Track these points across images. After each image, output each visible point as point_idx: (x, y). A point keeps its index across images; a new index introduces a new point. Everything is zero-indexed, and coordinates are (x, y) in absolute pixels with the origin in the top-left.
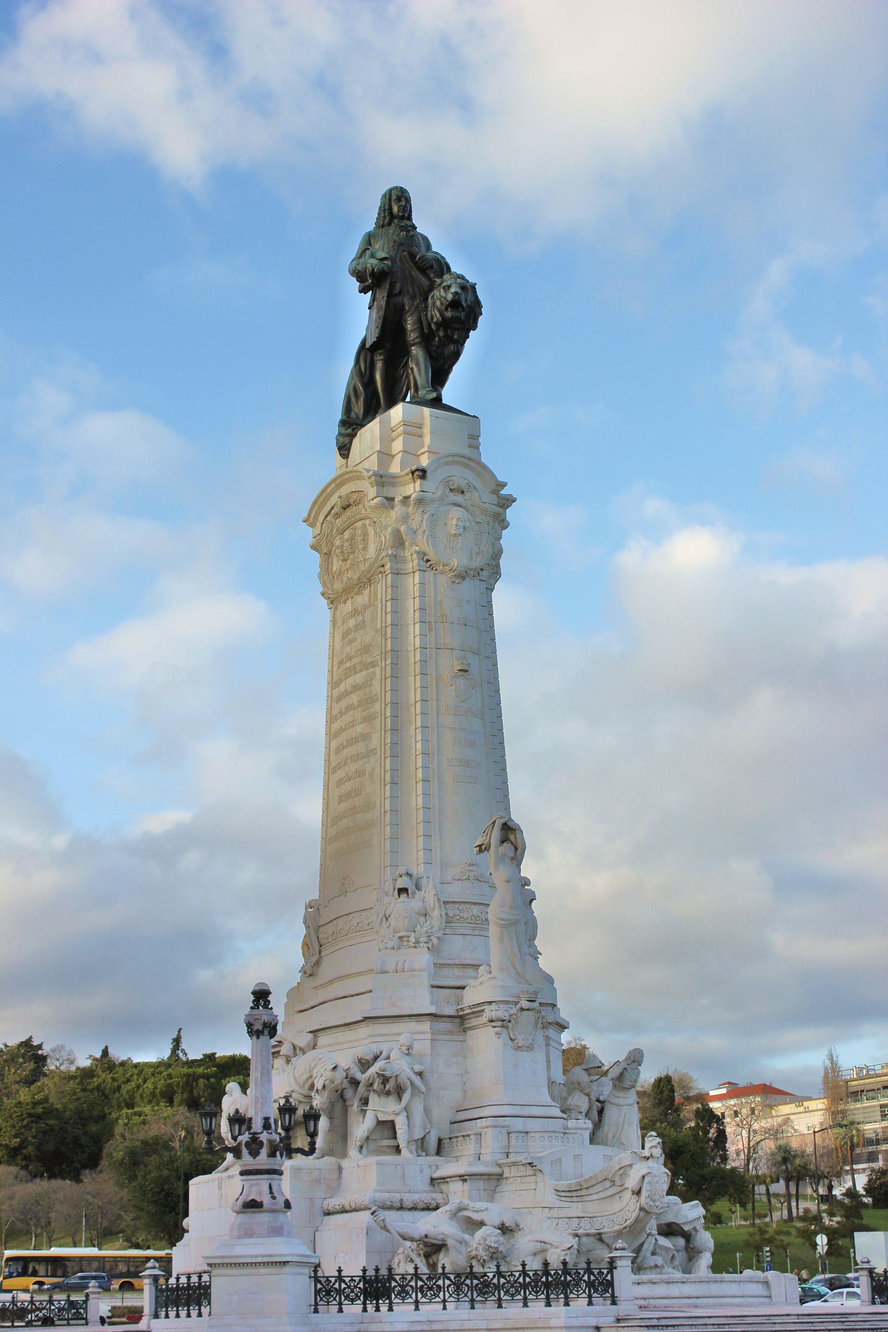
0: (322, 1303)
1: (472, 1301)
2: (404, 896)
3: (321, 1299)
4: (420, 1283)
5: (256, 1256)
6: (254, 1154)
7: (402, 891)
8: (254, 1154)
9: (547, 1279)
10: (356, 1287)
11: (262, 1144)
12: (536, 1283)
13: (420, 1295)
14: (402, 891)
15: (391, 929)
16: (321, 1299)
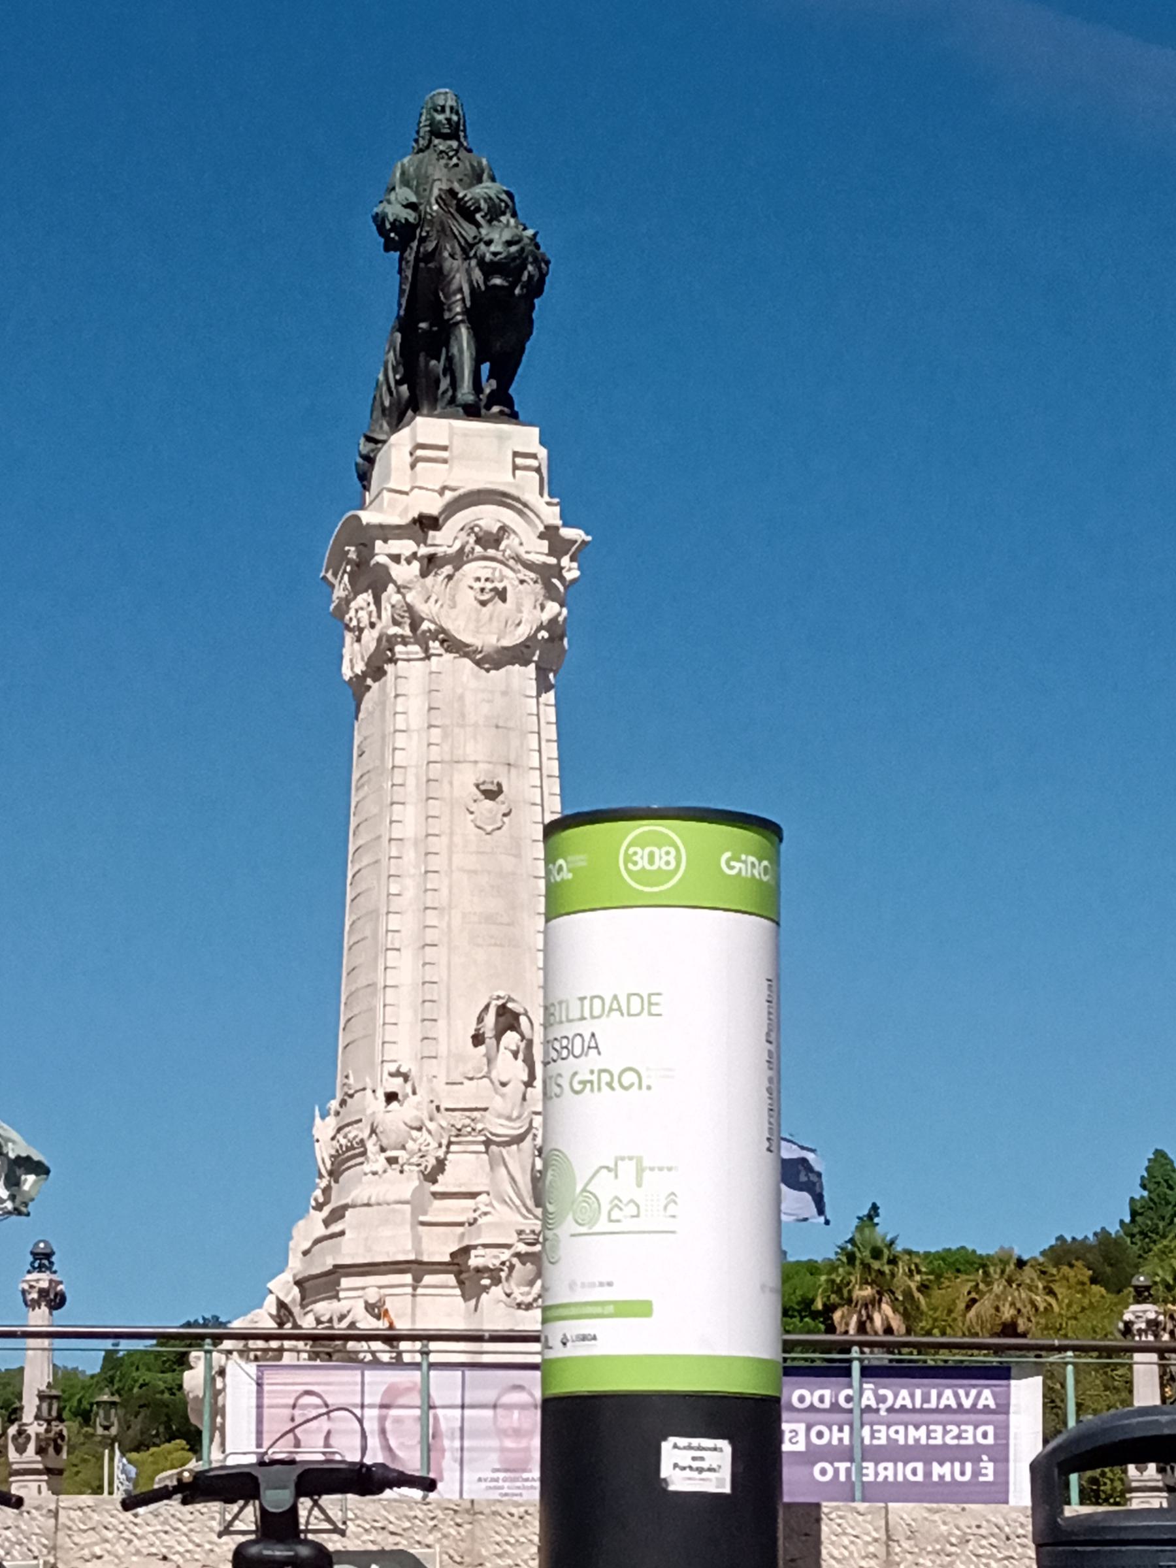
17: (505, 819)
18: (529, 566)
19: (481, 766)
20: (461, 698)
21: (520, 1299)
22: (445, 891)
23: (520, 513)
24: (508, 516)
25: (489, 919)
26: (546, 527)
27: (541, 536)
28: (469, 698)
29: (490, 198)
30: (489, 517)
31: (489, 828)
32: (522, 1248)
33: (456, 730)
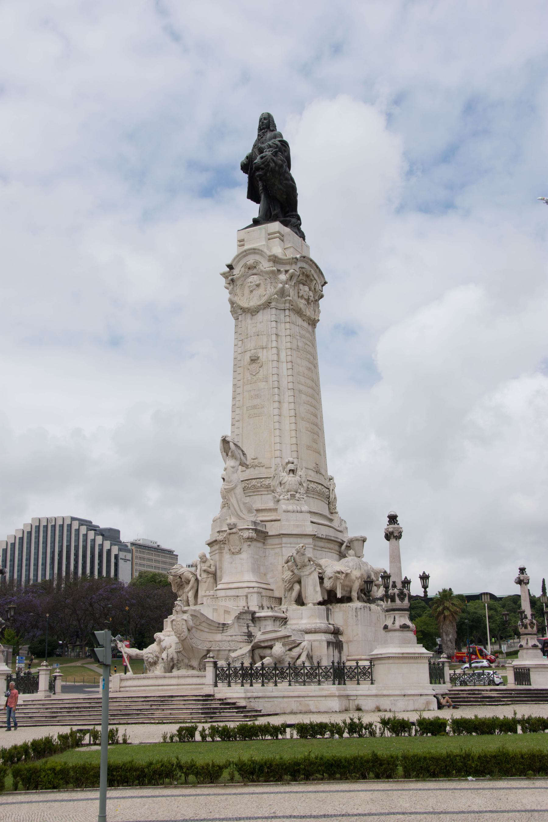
0: (361, 679)
1: (290, 681)
2: (291, 475)
3: (361, 678)
4: (306, 671)
5: (414, 654)
6: (402, 600)
7: (292, 471)
8: (402, 600)
9: (251, 672)
10: (353, 671)
11: (405, 595)
12: (257, 674)
13: (306, 677)
14: (292, 471)
15: (286, 490)
16: (361, 678)
17: (261, 369)
18: (267, 273)
19: (252, 351)
20: (247, 328)
21: (233, 551)
22: (241, 400)
23: (262, 255)
24: (257, 257)
25: (254, 407)
26: (269, 256)
27: (269, 261)
28: (249, 327)
29: (269, 145)
30: (250, 260)
31: (254, 374)
32: (229, 531)
33: (246, 340)
